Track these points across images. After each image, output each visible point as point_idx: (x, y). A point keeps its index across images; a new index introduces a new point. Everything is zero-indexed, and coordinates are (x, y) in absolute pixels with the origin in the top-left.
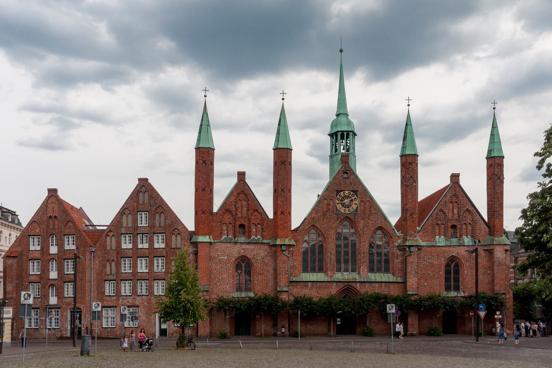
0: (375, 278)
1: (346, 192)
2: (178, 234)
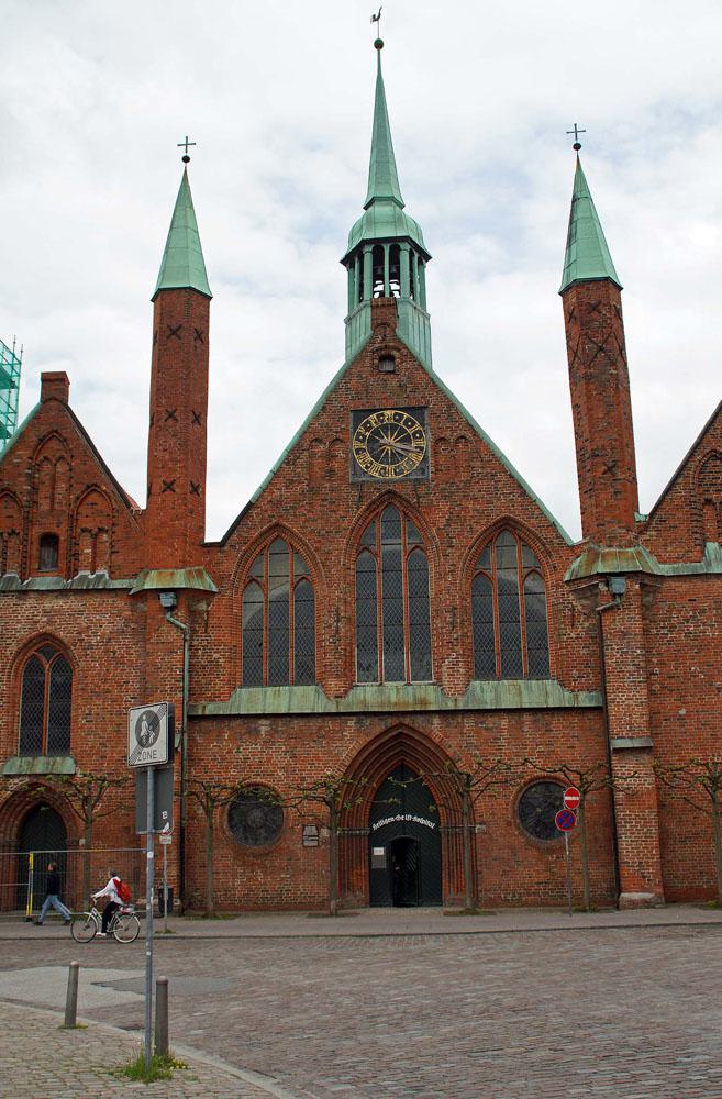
0: (497, 698)
1: (388, 413)
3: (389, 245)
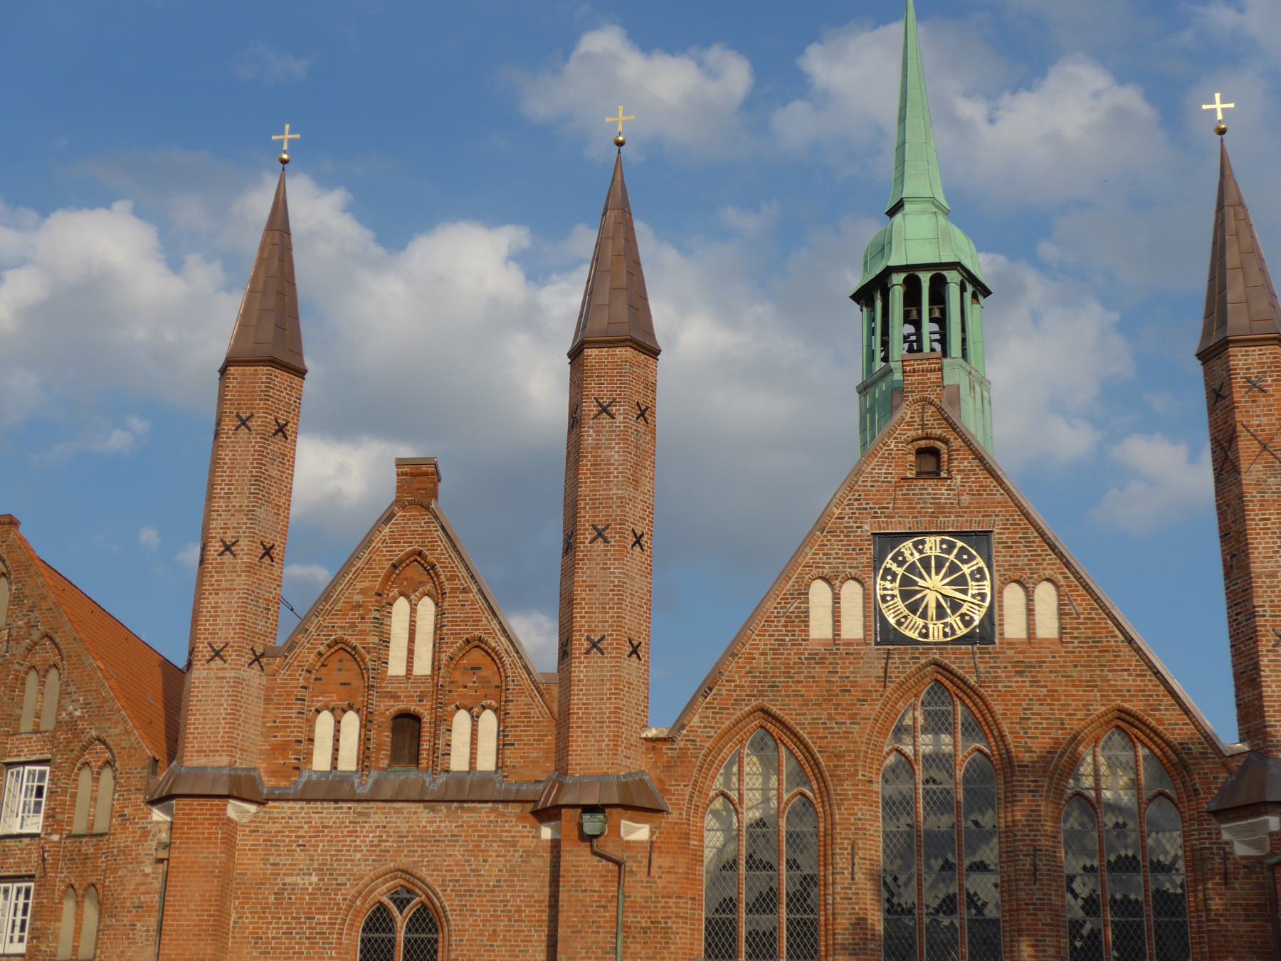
1: (930, 541)
2: (108, 762)
3: (929, 274)
